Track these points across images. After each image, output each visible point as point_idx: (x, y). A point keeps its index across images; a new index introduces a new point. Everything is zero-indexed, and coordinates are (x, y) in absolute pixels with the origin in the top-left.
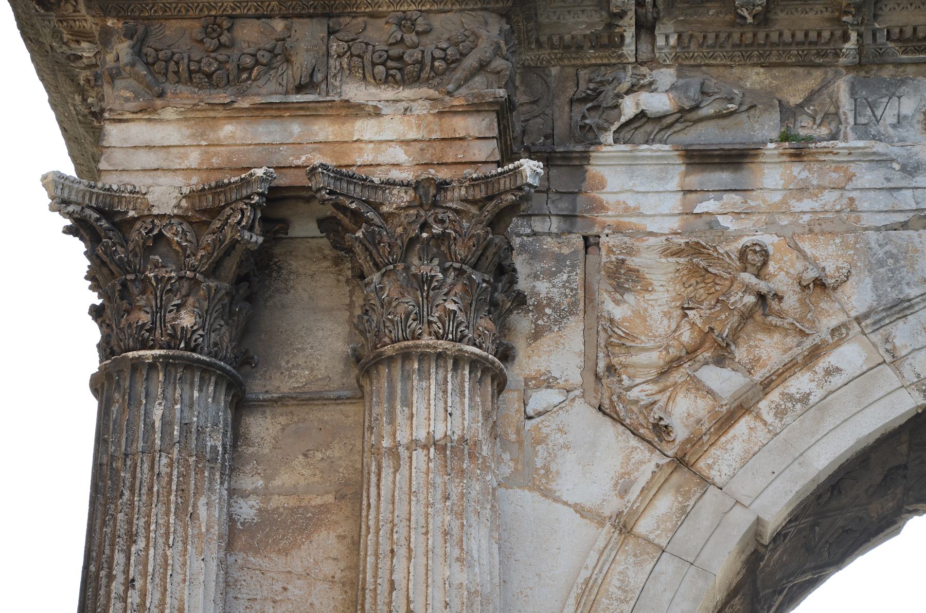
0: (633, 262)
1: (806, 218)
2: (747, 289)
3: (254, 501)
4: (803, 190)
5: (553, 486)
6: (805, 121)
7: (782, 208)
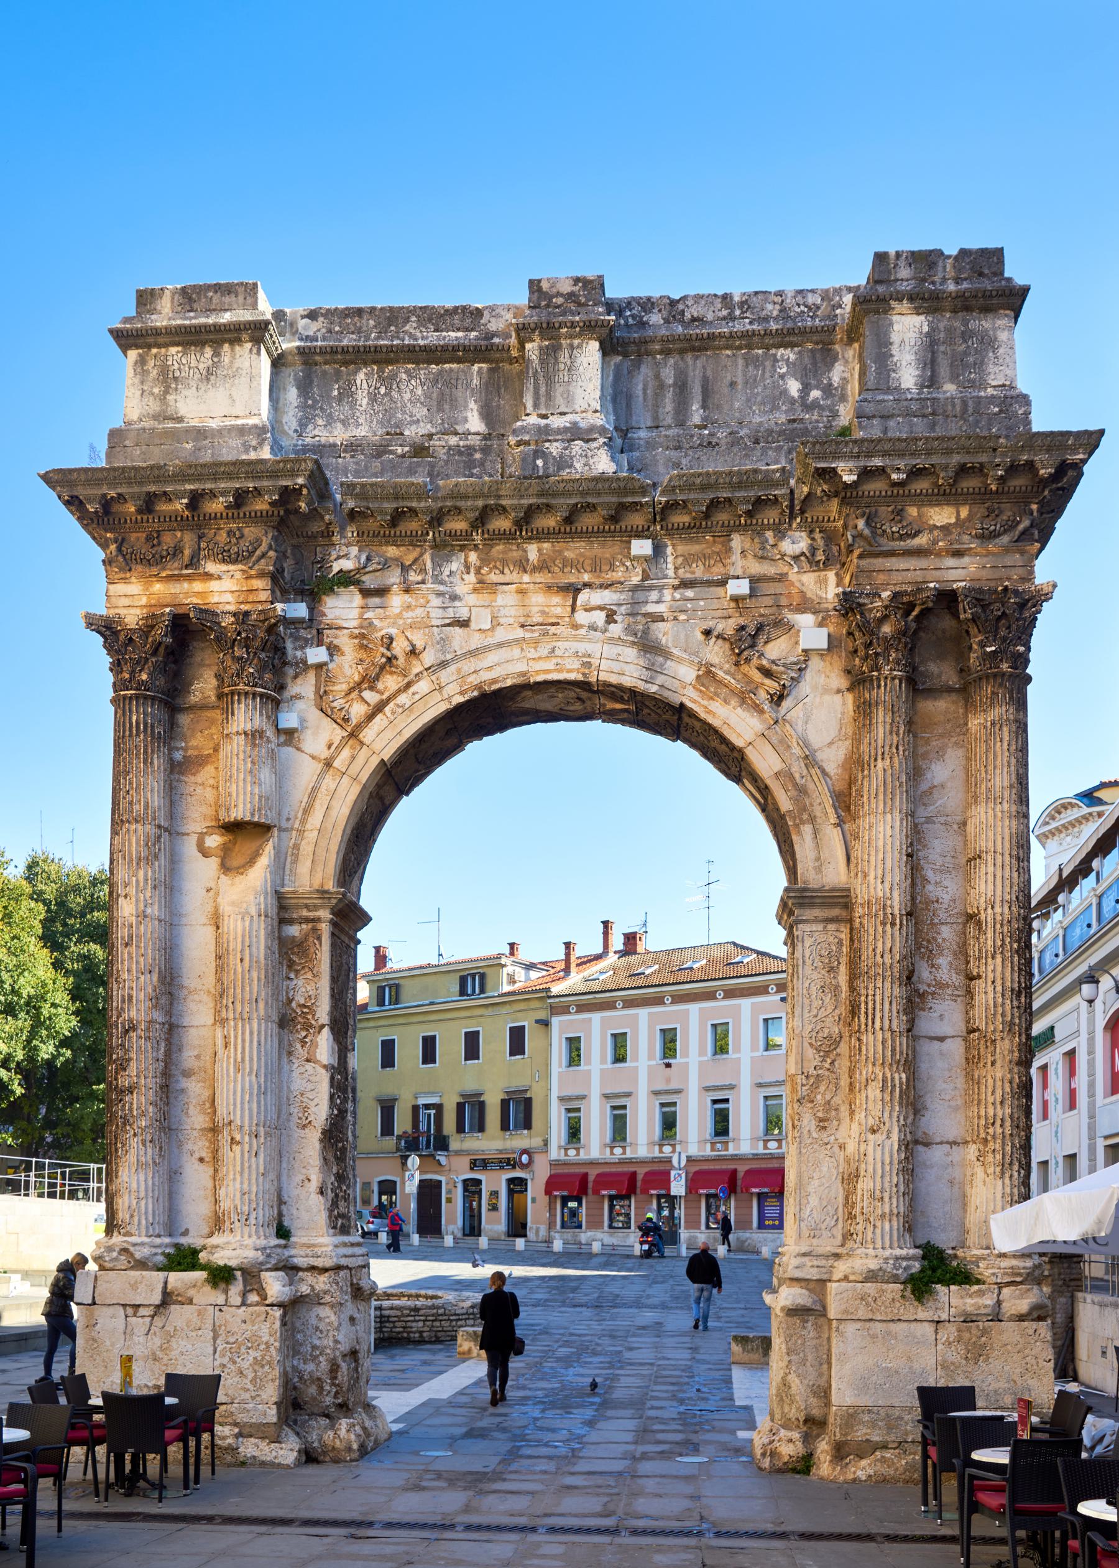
0: (336, 642)
1: (409, 621)
2: (383, 655)
3: (181, 752)
4: (409, 607)
5: (301, 746)
6: (412, 573)
7: (399, 616)
